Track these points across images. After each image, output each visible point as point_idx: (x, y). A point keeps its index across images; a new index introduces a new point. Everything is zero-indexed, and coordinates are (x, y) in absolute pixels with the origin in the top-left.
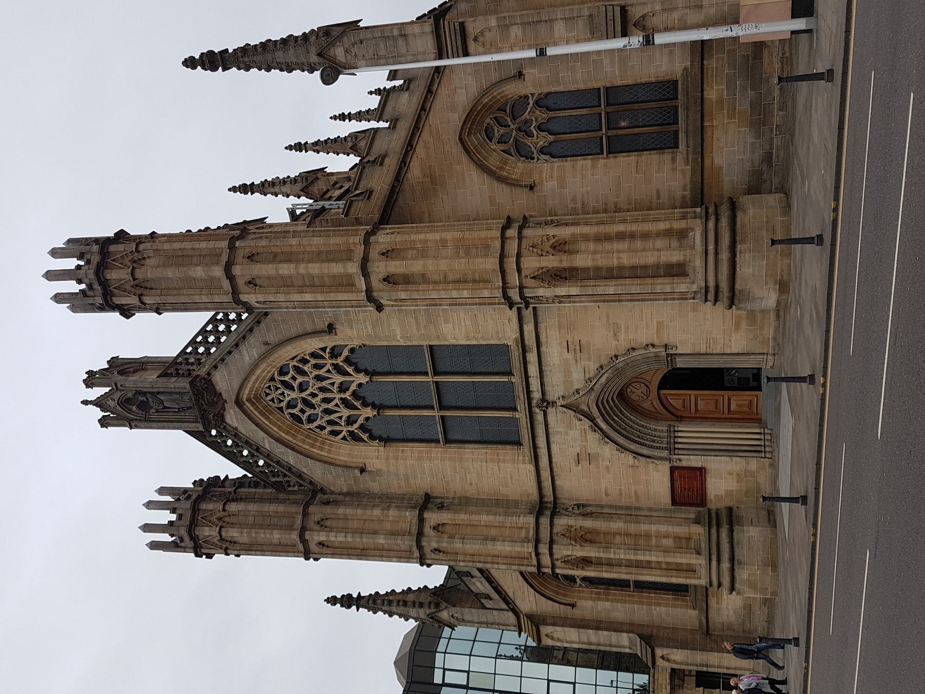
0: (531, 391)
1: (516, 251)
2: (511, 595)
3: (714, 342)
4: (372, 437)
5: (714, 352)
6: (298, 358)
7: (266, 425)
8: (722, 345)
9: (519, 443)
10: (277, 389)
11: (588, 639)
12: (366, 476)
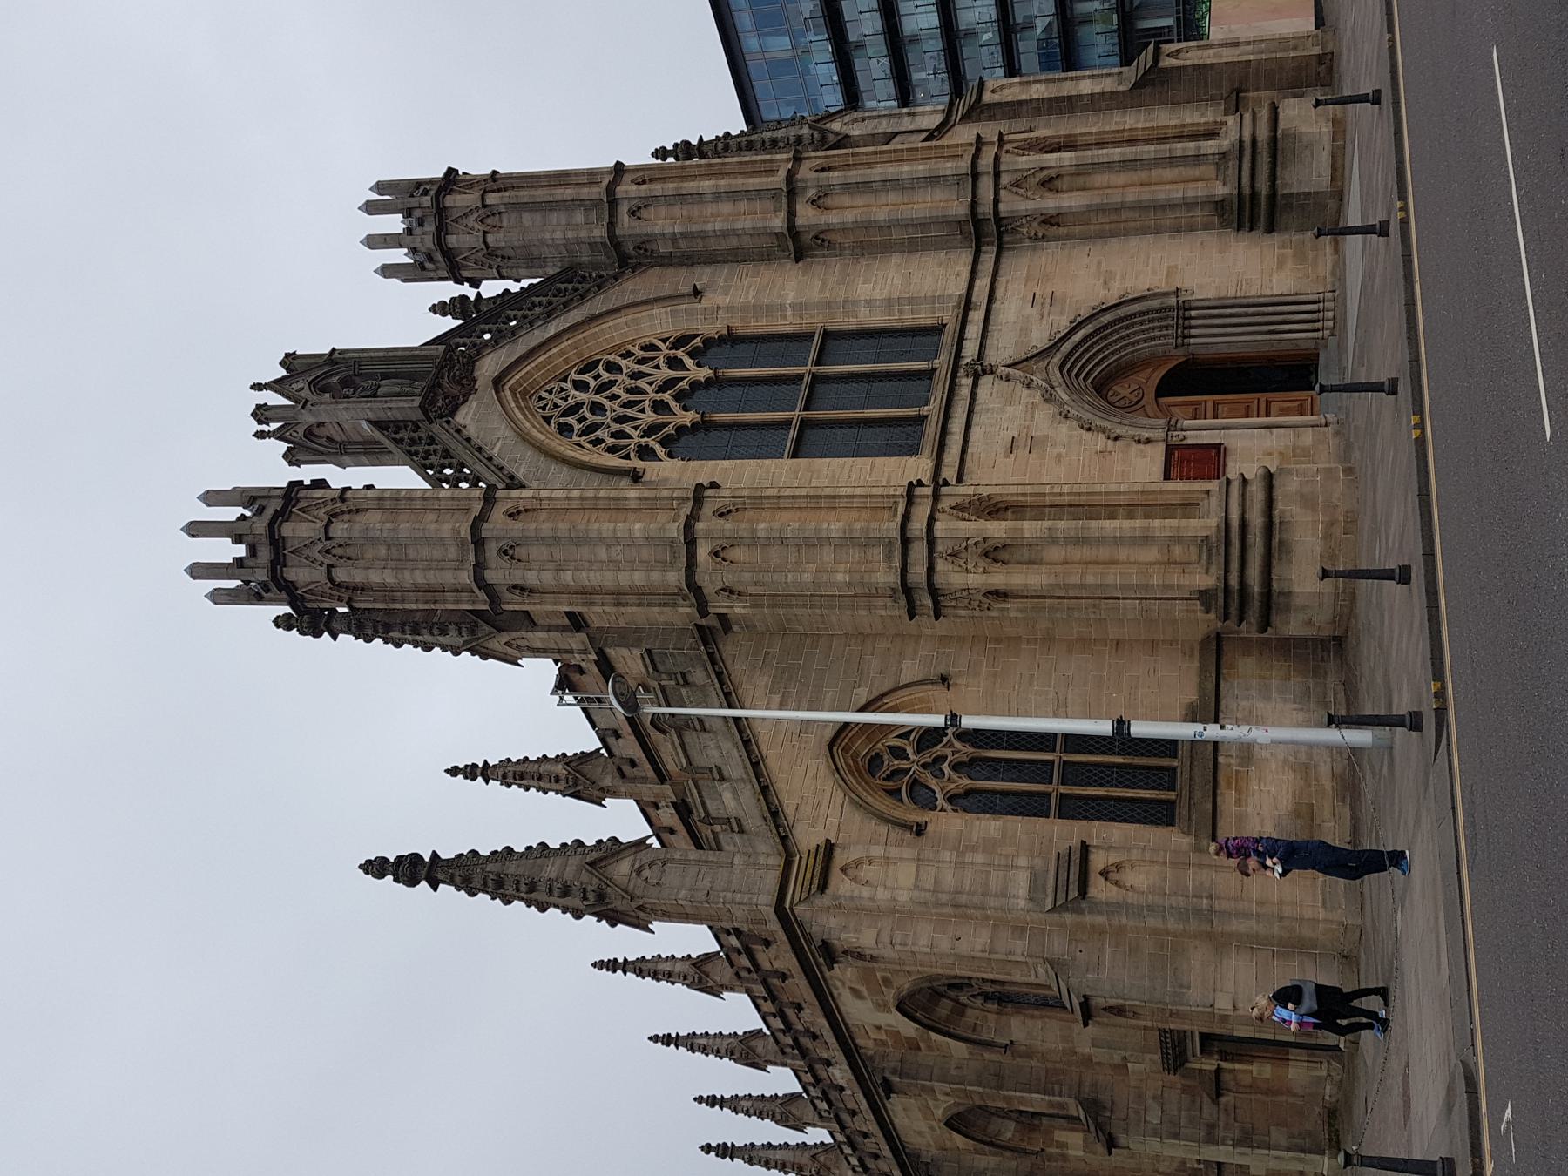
2: (790, 811)
4: (671, 456)
8: (1259, 287)
11: (936, 881)
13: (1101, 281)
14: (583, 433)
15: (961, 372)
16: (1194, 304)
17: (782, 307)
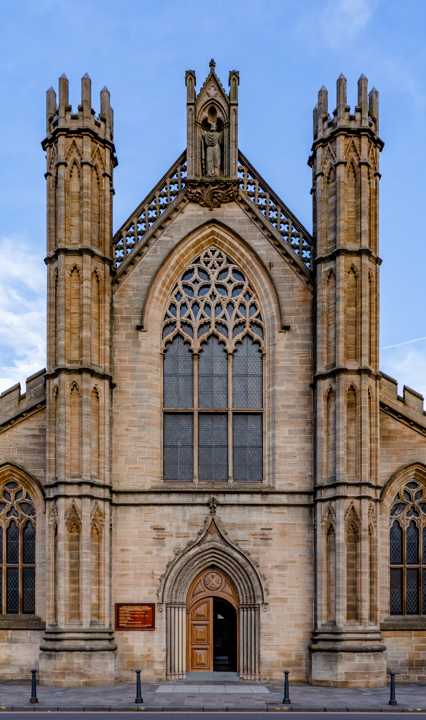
0: (225, 495)
1: (349, 495)
3: (269, 639)
5: (261, 639)
6: (251, 292)
7: (187, 244)
8: (267, 644)
9: (165, 477)
10: (220, 263)
12: (132, 331)
13: (278, 564)
14: (185, 286)
15: (212, 496)
16: (257, 612)
17: (274, 384)
